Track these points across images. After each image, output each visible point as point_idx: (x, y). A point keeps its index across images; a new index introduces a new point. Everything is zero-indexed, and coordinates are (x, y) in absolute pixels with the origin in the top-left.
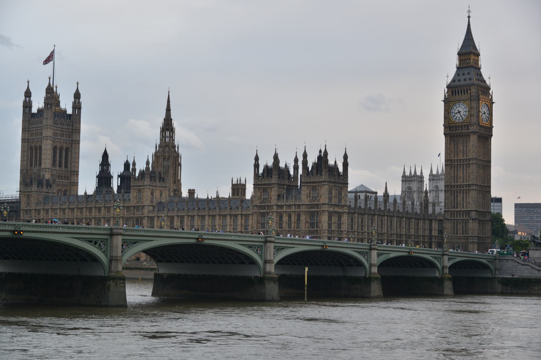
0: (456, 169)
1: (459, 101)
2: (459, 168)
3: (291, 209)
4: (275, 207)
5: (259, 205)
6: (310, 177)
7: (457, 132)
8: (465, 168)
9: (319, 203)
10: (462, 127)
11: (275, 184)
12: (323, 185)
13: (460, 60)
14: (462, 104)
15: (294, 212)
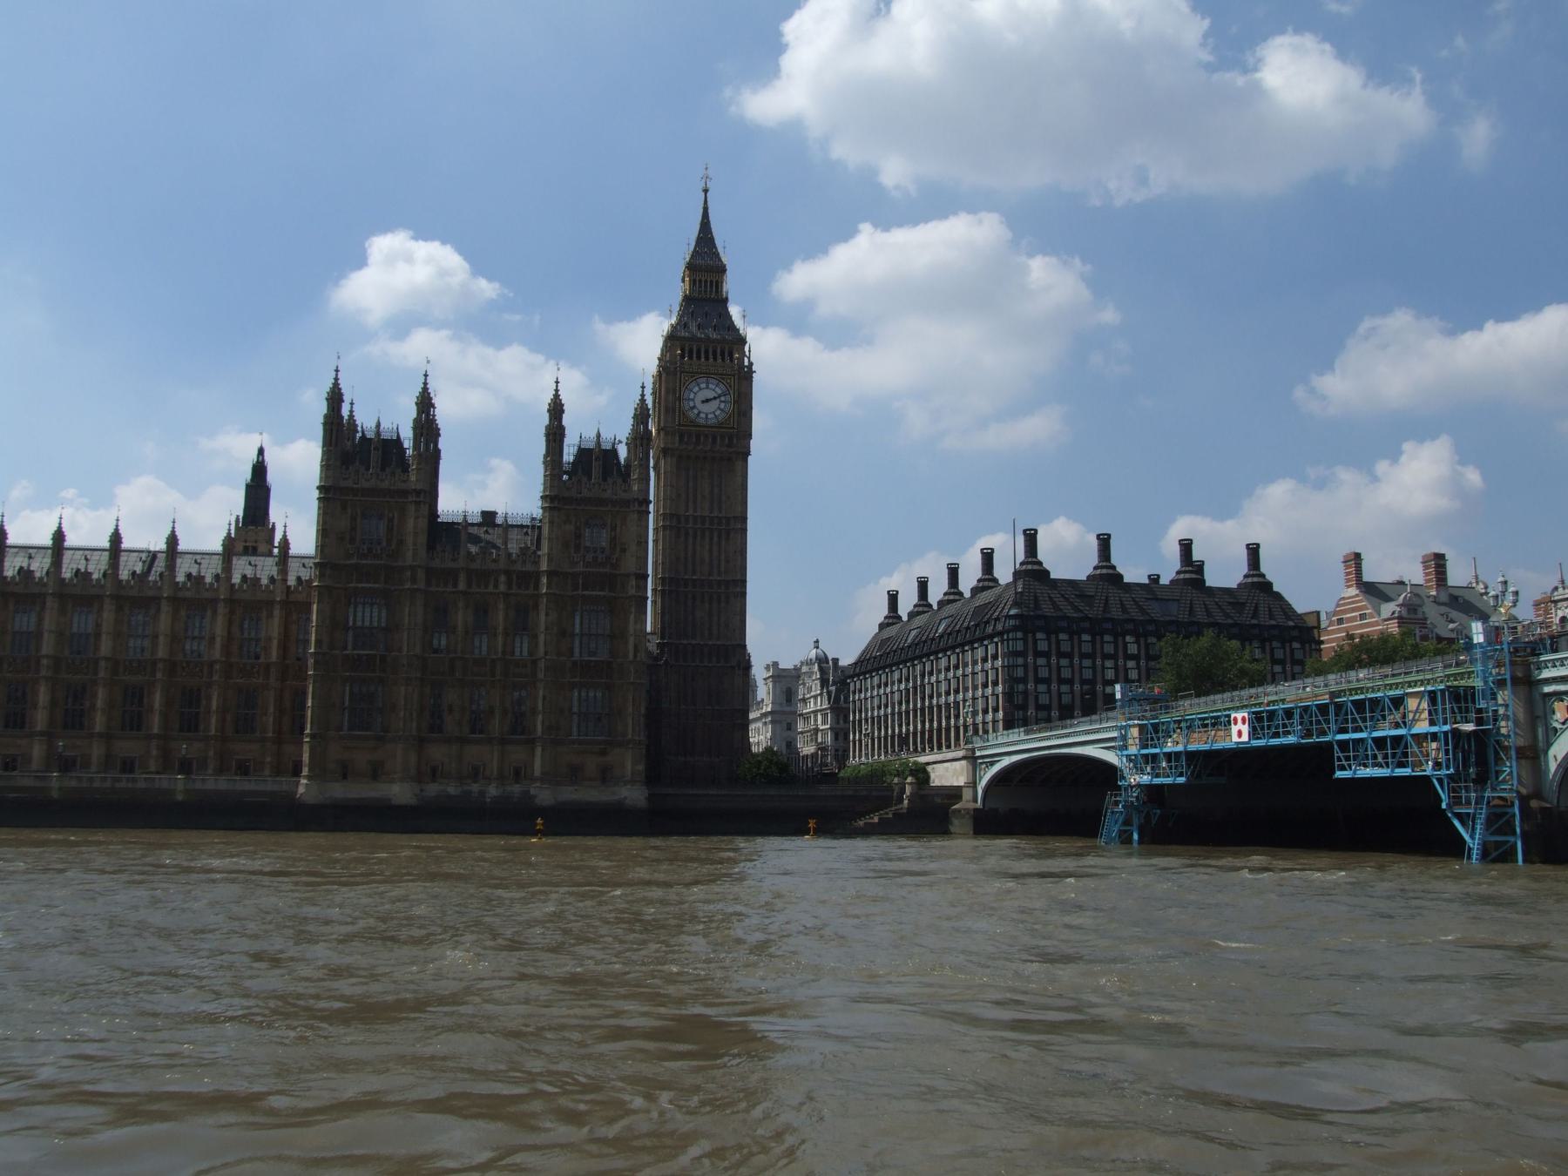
0: (691, 540)
1: (708, 375)
2: (699, 538)
3: (486, 587)
4: (421, 575)
5: (342, 562)
6: (579, 481)
7: (699, 448)
8: (716, 539)
9: (618, 572)
10: (714, 439)
11: (425, 492)
12: (639, 512)
13: (693, 282)
14: (716, 382)
15: (506, 595)
